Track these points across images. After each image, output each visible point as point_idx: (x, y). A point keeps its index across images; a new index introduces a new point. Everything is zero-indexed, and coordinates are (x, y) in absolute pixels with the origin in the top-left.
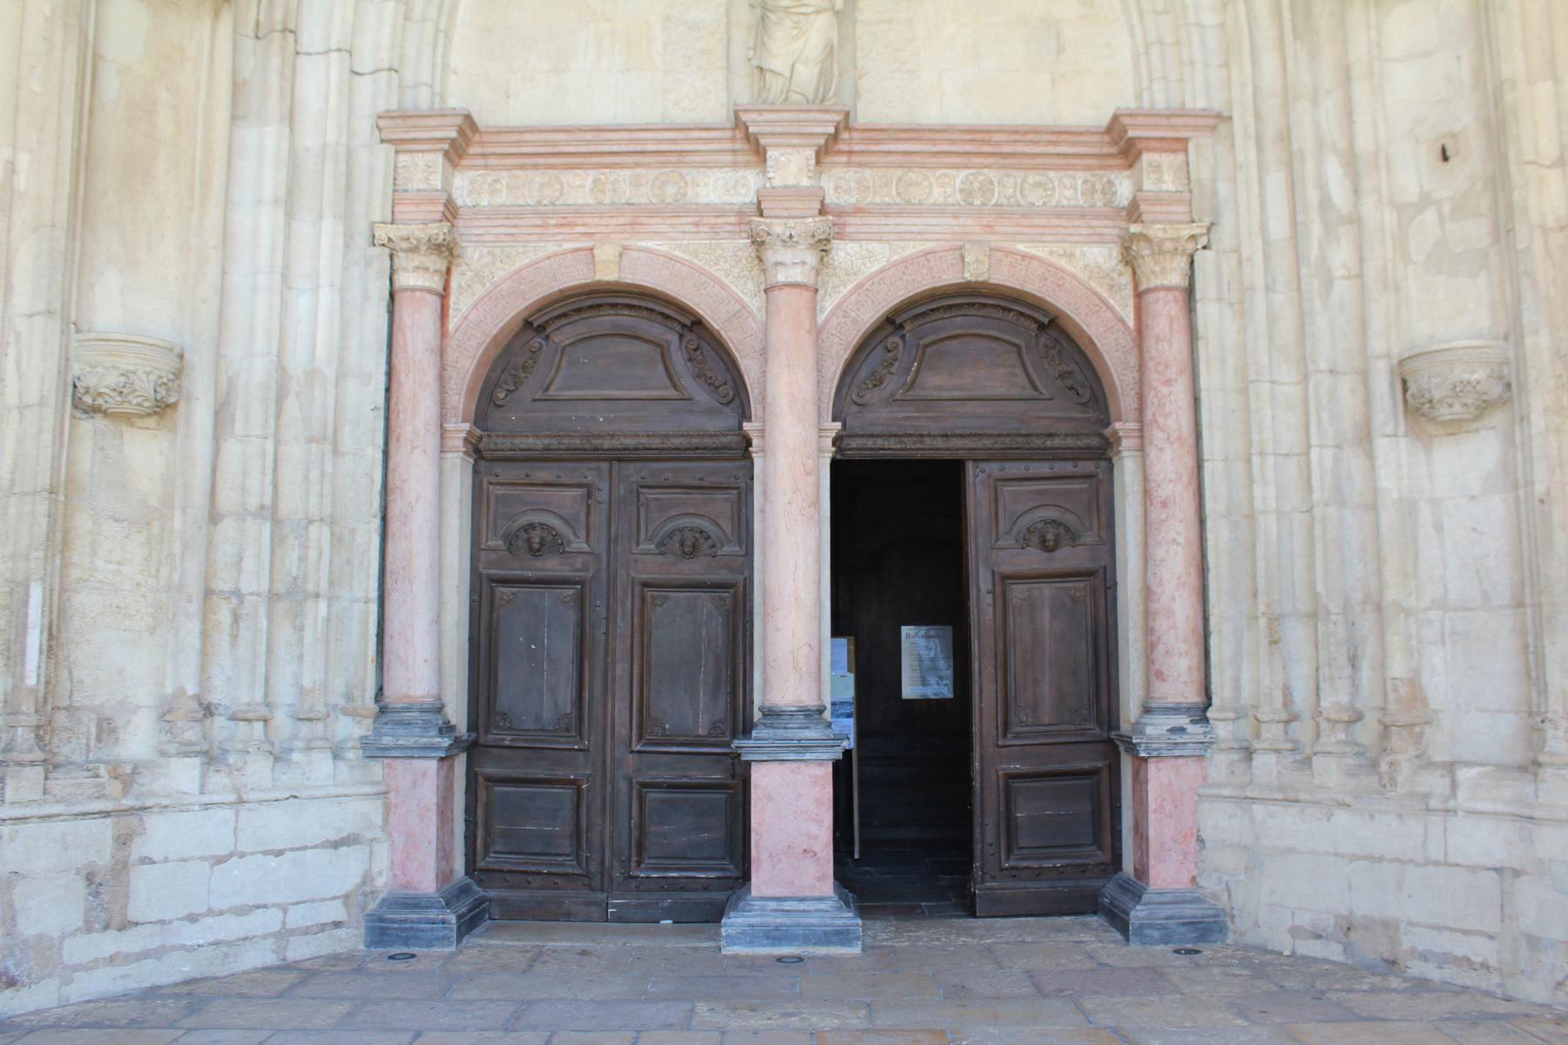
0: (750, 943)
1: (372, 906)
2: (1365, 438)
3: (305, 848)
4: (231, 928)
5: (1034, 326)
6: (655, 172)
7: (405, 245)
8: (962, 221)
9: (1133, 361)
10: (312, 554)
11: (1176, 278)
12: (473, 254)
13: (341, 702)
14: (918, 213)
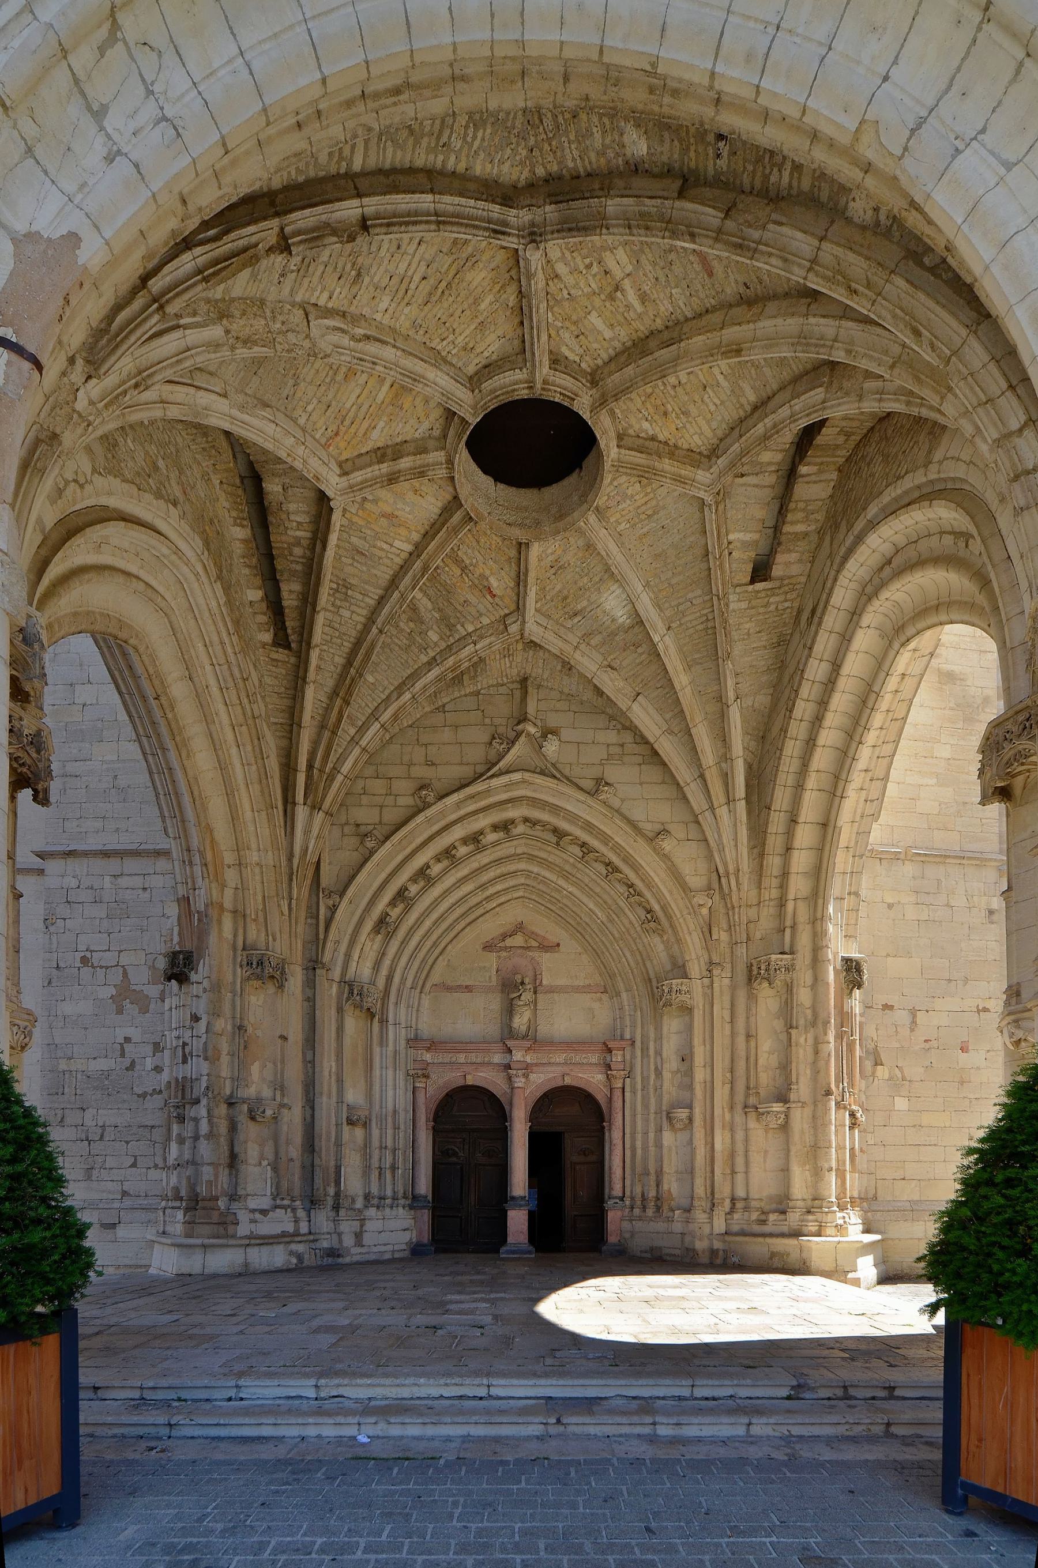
4: (383, 1249)
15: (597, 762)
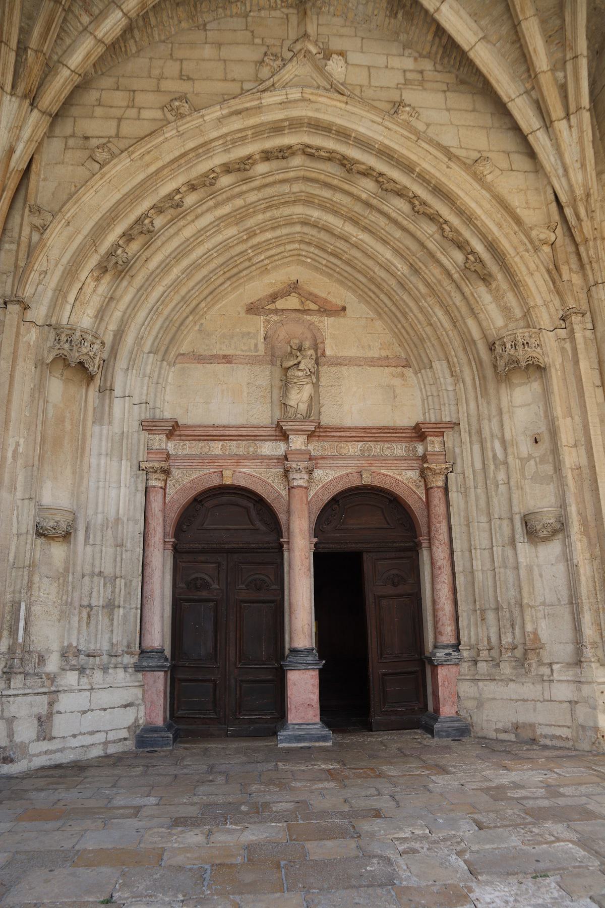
0: (289, 742)
1: (138, 732)
2: (513, 543)
3: (115, 708)
4: (88, 740)
5: (388, 501)
6: (245, 443)
7: (151, 470)
8: (361, 462)
9: (425, 514)
10: (117, 590)
11: (441, 483)
12: (175, 473)
13: (126, 649)
14: (345, 459)
15: (393, 85)
